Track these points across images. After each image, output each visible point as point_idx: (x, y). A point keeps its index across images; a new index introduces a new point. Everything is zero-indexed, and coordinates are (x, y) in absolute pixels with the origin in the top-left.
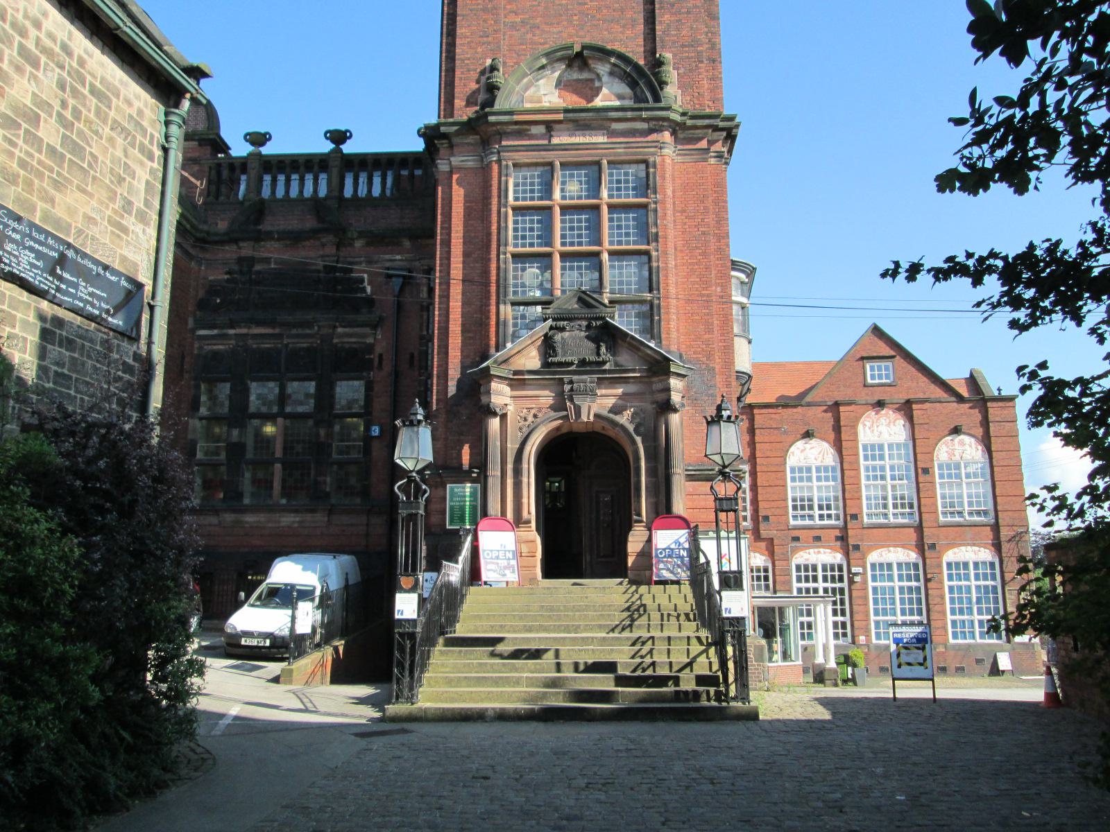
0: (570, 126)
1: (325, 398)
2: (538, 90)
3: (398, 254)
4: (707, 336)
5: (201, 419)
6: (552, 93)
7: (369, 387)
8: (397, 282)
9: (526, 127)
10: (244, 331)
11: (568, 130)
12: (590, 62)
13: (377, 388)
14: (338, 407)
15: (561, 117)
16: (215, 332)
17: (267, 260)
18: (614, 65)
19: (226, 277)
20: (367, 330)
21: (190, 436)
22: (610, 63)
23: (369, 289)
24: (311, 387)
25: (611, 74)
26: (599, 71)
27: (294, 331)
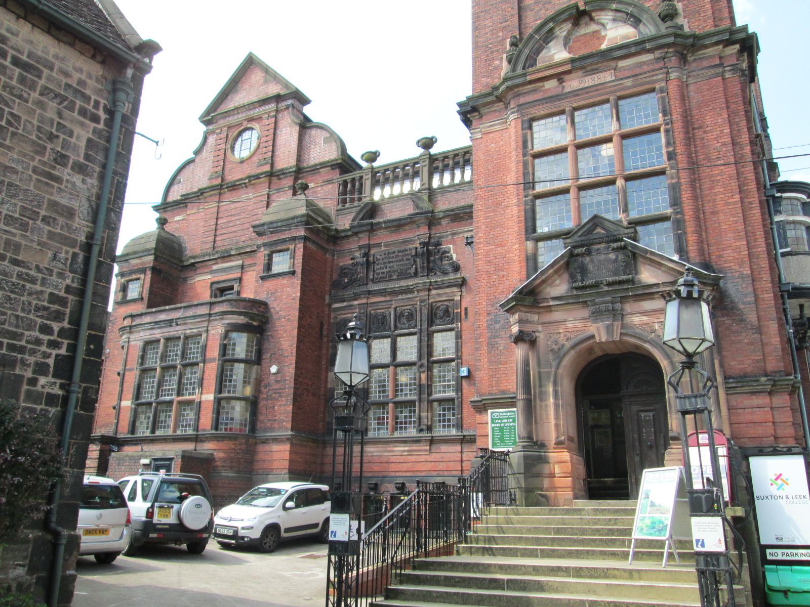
0: (580, 73)
2: (549, 51)
4: (738, 244)
6: (562, 51)
7: (459, 337)
9: (541, 84)
10: (364, 301)
11: (579, 77)
12: (594, 14)
14: (435, 354)
15: (568, 67)
18: (617, 11)
19: (351, 262)
20: (455, 289)
21: (329, 386)
22: (612, 10)
23: (454, 256)
24: (414, 340)
25: (614, 20)
26: (602, 21)
27: (400, 297)
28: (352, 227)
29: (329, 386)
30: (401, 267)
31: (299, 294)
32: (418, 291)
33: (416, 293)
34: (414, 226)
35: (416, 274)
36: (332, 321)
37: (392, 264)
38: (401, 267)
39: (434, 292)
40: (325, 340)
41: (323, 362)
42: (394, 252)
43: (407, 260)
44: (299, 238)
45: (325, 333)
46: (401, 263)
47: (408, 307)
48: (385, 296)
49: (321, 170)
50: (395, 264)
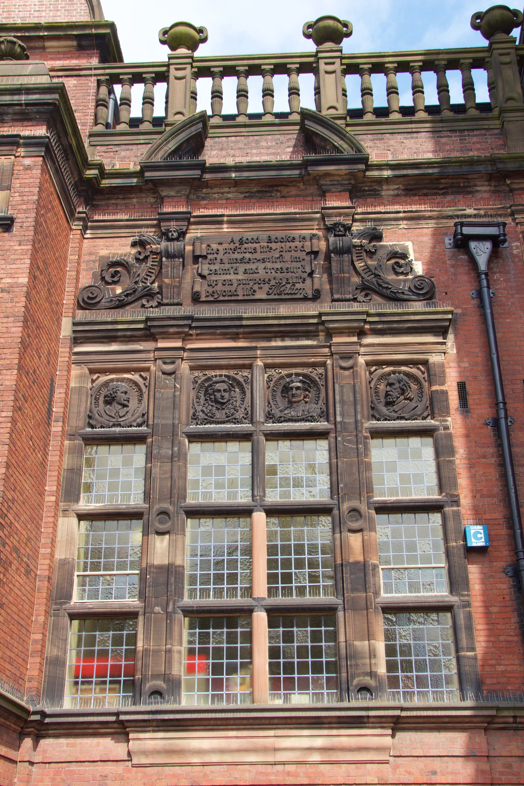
1: (349, 477)
3: (469, 206)
5: (81, 517)
7: (443, 452)
8: (482, 252)
13: (460, 447)
16: (114, 347)
17: (215, 221)
19: (134, 251)
21: (59, 555)
28: (145, 168)
29: (59, 555)
30: (279, 275)
31: (24, 280)
32: (330, 334)
33: (322, 336)
34: (313, 189)
35: (316, 296)
36: (72, 384)
37: (253, 266)
38: (279, 275)
39: (368, 340)
40: (56, 428)
41: (51, 487)
42: (257, 241)
43: (297, 260)
44: (31, 142)
45: (57, 409)
46: (278, 265)
47: (299, 370)
48: (235, 337)
49: (48, 44)
50: (261, 266)
